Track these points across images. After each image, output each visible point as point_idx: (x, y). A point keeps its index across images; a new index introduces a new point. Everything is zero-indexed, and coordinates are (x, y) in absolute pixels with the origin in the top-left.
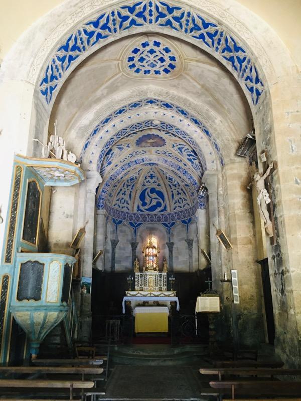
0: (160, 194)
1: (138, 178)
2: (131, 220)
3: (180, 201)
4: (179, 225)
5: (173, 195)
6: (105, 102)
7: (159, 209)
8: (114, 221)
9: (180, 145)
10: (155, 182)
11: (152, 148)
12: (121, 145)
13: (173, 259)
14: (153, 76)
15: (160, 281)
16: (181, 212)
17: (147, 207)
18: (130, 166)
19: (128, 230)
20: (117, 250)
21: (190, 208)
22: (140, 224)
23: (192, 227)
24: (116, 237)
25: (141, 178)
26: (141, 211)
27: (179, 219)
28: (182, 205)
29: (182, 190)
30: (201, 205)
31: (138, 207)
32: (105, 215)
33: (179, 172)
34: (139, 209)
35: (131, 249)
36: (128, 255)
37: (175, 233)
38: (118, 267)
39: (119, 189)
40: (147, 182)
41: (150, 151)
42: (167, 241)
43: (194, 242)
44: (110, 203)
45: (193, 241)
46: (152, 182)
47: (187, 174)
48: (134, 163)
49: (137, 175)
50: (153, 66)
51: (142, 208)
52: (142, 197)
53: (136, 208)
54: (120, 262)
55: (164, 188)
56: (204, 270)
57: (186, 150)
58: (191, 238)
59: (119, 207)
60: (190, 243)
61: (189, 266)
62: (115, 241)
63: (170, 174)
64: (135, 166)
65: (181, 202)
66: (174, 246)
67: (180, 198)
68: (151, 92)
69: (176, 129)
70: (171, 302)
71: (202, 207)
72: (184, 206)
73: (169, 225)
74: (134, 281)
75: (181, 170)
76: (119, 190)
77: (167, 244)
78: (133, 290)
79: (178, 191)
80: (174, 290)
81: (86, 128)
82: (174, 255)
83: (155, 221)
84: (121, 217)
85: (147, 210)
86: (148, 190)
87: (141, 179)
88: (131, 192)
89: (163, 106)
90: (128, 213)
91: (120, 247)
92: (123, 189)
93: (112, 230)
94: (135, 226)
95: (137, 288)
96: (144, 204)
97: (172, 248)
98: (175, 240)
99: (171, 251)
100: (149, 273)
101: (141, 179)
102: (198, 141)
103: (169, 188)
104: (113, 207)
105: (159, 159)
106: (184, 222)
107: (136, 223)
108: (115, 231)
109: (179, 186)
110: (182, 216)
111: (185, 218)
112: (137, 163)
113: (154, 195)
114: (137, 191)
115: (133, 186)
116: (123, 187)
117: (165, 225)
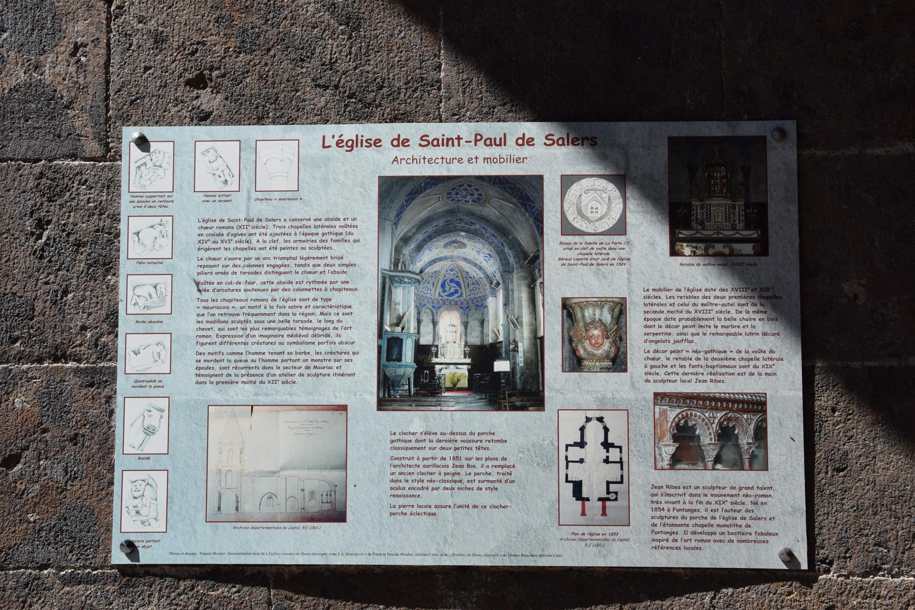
0: (458, 284)
7: (457, 295)
34: (440, 295)
50: (465, 197)
51: (442, 294)
52: (443, 286)
53: (437, 295)
98: (470, 320)
101: (443, 272)
106: (477, 306)
113: (453, 284)
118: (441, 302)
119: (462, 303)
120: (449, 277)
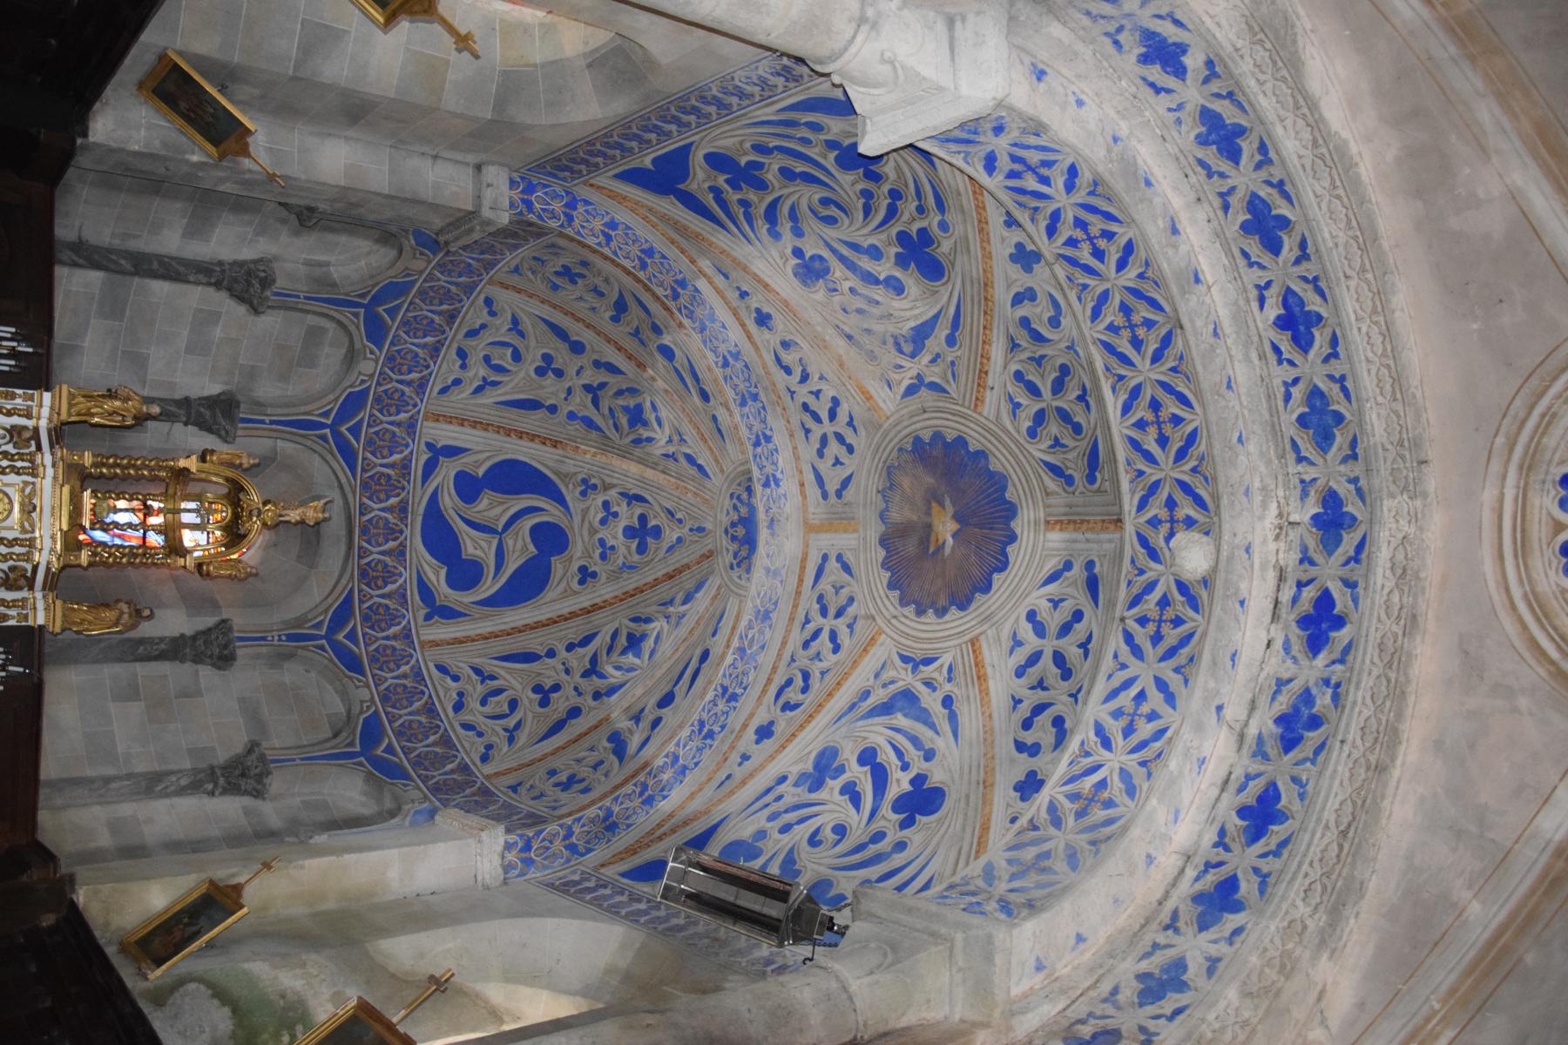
0: (527, 584)
1: (637, 452)
2: (377, 400)
3: (499, 704)
4: (344, 694)
5: (529, 657)
6: (1392, 217)
7: (437, 576)
8: (395, 290)
9: (947, 702)
10: (606, 552)
11: (874, 530)
12: (951, 341)
13: (118, 669)
14: (1539, 531)
16: (430, 710)
17: (450, 502)
18: (743, 403)
19: (319, 382)
20: (195, 296)
21: (464, 768)
22: (348, 455)
23: (348, 790)
24: (288, 303)
25: (634, 468)
26: (430, 469)
27: (385, 699)
28: (475, 712)
29: (575, 712)
30: (527, 847)
31: (453, 451)
32: (472, 215)
33: (710, 696)
36: (157, 365)
37: (291, 674)
38: (74, 287)
39: (586, 336)
40: (606, 505)
41: (840, 521)
42: (241, 621)
43: (247, 801)
44: (517, 270)
45: (258, 794)
46: (603, 533)
47: (697, 743)
48: (757, 427)
49: (658, 449)
51: (447, 472)
52: (512, 477)
53: (447, 434)
54: (113, 308)
57: (915, 741)
58: (275, 783)
59: (472, 333)
60: (242, 774)
61: (76, 782)
62: (267, 282)
63: (668, 641)
64: (744, 432)
65: (487, 709)
66: (206, 673)
67: (513, 704)
68: (1414, 518)
69: (1161, 685)
71: (511, 857)
72: (467, 727)
73: (340, 637)
75: (722, 705)
76: (578, 332)
79: (556, 688)
81: (1287, 63)
82: (142, 670)
83: (363, 553)
84: (411, 343)
85: (434, 495)
86: (551, 513)
87: (628, 472)
88: (553, 409)
89: (1309, 593)
90: (421, 386)
91: (214, 317)
92: (585, 360)
93: (336, 273)
96: (468, 487)
97: (197, 660)
99: (175, 650)
100: (49, 488)
101: (628, 472)
102: (1136, 841)
103: (573, 631)
104: (485, 289)
105: (776, 573)
106: (372, 731)
107: (356, 431)
108: (326, 295)
109: (597, 696)
110: (404, 715)
111: (399, 734)
112: (757, 444)
113: (520, 549)
114: (555, 444)
115: (589, 423)
116: (597, 364)
117: (343, 614)
118: (380, 464)
120: (581, 519)
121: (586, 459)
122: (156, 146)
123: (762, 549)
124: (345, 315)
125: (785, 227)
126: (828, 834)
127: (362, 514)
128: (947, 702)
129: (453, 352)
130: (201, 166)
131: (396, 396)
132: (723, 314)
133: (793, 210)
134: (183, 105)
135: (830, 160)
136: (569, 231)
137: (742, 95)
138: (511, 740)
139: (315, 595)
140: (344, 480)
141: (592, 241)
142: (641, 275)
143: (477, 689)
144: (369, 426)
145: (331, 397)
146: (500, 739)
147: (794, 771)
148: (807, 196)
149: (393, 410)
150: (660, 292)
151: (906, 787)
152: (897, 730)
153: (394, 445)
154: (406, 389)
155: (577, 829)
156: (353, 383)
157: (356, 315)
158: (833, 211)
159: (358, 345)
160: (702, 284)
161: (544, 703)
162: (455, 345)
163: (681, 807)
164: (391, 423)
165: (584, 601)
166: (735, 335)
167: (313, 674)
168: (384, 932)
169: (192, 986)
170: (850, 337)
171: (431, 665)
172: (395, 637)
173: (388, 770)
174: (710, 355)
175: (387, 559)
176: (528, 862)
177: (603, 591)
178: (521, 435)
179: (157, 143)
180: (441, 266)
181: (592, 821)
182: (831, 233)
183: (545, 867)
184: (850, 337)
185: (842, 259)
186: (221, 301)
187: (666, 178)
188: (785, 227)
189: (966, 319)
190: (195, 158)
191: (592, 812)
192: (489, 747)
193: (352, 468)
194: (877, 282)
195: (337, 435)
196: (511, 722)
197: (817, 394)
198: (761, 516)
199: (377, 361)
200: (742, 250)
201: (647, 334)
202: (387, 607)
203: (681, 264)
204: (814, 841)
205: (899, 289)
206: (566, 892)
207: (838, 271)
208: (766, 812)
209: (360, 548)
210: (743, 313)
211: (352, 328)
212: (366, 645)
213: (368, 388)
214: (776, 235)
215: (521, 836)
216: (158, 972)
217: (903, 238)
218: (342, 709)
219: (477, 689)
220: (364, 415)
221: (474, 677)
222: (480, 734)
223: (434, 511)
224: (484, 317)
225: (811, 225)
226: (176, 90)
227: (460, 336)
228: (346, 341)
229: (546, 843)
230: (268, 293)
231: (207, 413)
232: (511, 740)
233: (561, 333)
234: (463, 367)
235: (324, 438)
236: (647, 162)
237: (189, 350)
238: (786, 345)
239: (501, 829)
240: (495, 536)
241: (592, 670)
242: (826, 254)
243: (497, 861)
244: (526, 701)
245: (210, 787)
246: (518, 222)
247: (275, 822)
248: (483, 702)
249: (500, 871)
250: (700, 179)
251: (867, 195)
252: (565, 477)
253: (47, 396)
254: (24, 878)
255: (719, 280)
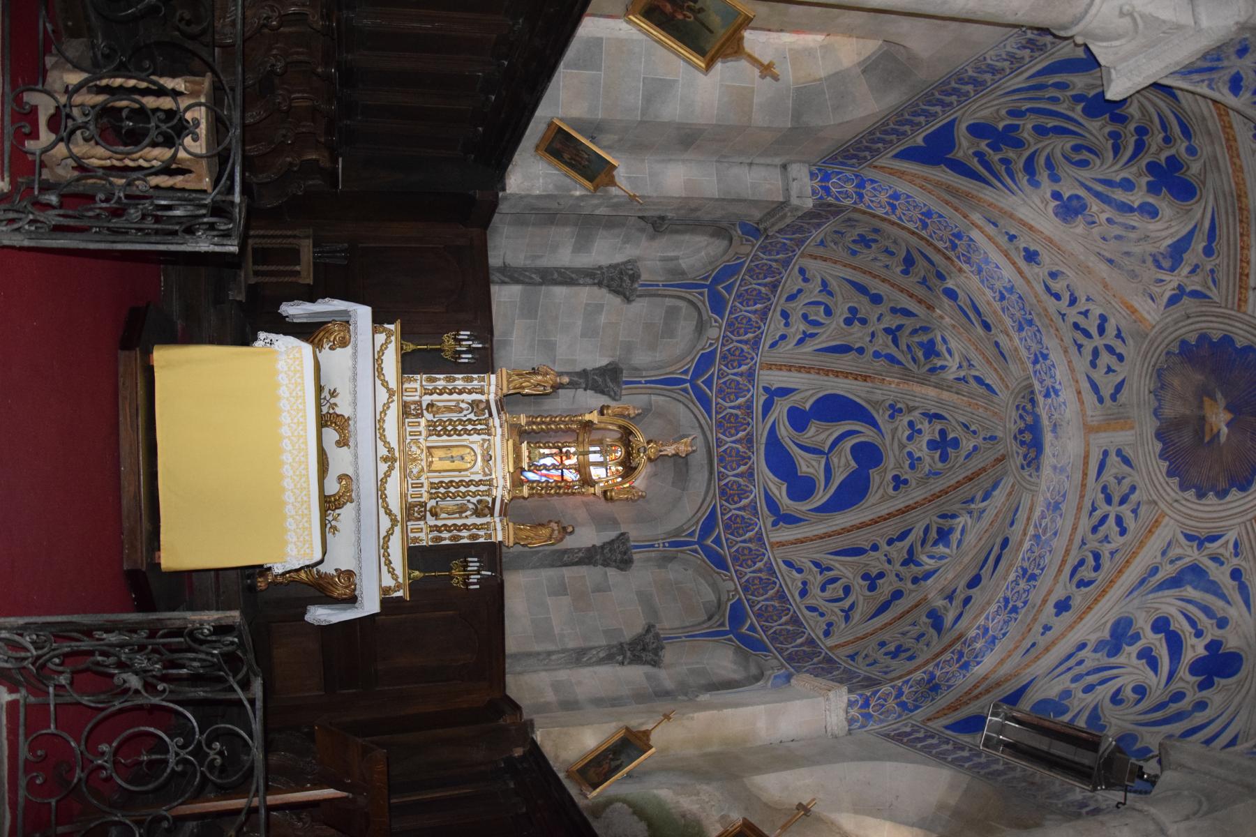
0: (852, 492)
1: (933, 378)
2: (724, 357)
3: (836, 590)
4: (714, 586)
5: (857, 552)
7: (780, 491)
8: (729, 271)
10: (914, 462)
11: (1150, 426)
12: (1208, 251)
15: (461, 510)
16: (781, 596)
17: (785, 432)
18: (1021, 329)
19: (677, 350)
20: (585, 294)
21: (811, 642)
22: (705, 401)
23: (722, 660)
24: (651, 292)
25: (932, 392)
27: (746, 589)
28: (816, 597)
29: (897, 595)
30: (866, 704)
31: (785, 392)
32: (783, 205)
33: (1012, 577)
34: (775, 394)
35: (589, 367)
36: (562, 351)
37: (673, 573)
38: (504, 297)
40: (911, 424)
43: (648, 669)
44: (822, 243)
45: (655, 663)
48: (1035, 347)
49: (951, 374)
51: (781, 409)
52: (833, 408)
53: (779, 379)
54: (529, 309)
55: (884, 509)
56: (535, 751)
57: (1207, 610)
58: (668, 655)
59: (791, 298)
60: (643, 649)
61: (529, 655)
62: (634, 277)
63: (972, 533)
64: (1024, 353)
65: (827, 594)
66: (612, 573)
67: (847, 590)
70: (350, 574)
72: (812, 609)
73: (709, 542)
74: (452, 366)
75: (1023, 584)
76: (876, 287)
77: (623, 537)
78: (409, 364)
79: (881, 575)
80: (414, 586)
82: (567, 572)
83: (722, 476)
84: (745, 311)
85: (773, 430)
86: (867, 434)
87: (926, 395)
88: (861, 351)
90: (756, 344)
91: (599, 308)
92: (882, 308)
93: (684, 264)
94: (697, 381)
95: (418, 382)
97: (606, 564)
98: (642, 575)
99: (589, 557)
100: (500, 443)
103: (892, 528)
104: (798, 262)
105: (1062, 470)
106: (737, 615)
107: (709, 383)
108: (679, 282)
109: (915, 580)
112: (1035, 362)
113: (844, 464)
114: (865, 378)
115: (891, 359)
116: (894, 310)
117: (709, 524)
119: (737, 526)
121: (891, 388)
122: (551, 189)
123: (1048, 450)
124: (693, 295)
125: (1043, 176)
126: (1128, 693)
127: (718, 446)
128: (1236, 574)
129: (778, 313)
130: (581, 198)
131: (737, 353)
132: (996, 256)
133: (1048, 159)
134: (566, 156)
135: (1077, 112)
136: (861, 206)
137: (993, 70)
138: (847, 618)
139: (687, 511)
140: (703, 422)
141: (880, 212)
142: (923, 233)
143: (817, 579)
144: (719, 378)
145: (689, 359)
146: (838, 618)
147: (1093, 639)
148: (1060, 146)
149: (735, 364)
150: (940, 245)
151: (1201, 651)
152: (1189, 601)
153: (739, 391)
154: (745, 347)
155: (906, 690)
156: (703, 347)
157: (701, 294)
158: (1085, 155)
159: (705, 317)
160: (975, 234)
161: (872, 588)
162: (779, 309)
163: (994, 671)
164: (735, 374)
165: (900, 503)
166: (1008, 272)
167: (690, 572)
168: (758, 769)
169: (619, 805)
170: (1110, 261)
171: (780, 561)
172: (750, 540)
173: (751, 644)
174: (988, 292)
175: (740, 480)
176: (867, 717)
177: (915, 494)
178: (837, 374)
179: (551, 186)
180: (763, 249)
181: (918, 683)
182: (1084, 174)
183: (881, 721)
184: (1110, 261)
185: (1098, 195)
186: (603, 296)
187: (937, 150)
188: (1043, 176)
189: (1222, 231)
190: (578, 193)
191: (918, 675)
192: (830, 625)
193: (709, 412)
194: (1131, 209)
195: (695, 387)
196: (846, 604)
197: (1085, 314)
198: (1045, 422)
199: (720, 328)
200: (1008, 201)
201: (934, 281)
202: (743, 517)
203: (955, 220)
204: (1116, 699)
205: (1152, 212)
206: (901, 742)
207: (1095, 206)
208: (1070, 675)
209: (719, 473)
210: (1013, 254)
211: (700, 304)
212: (729, 548)
213: (716, 349)
214: (1035, 184)
215: (861, 695)
216: (595, 793)
217: (1152, 167)
218: (712, 597)
219: (817, 579)
220: (714, 370)
221: (815, 569)
222: (822, 615)
223: (773, 441)
224: (800, 284)
225: (1066, 170)
226: (561, 146)
227: (783, 300)
228: (696, 314)
229: (881, 701)
230: (636, 285)
231: (600, 380)
232: (847, 618)
233: (862, 289)
234: (787, 324)
235: (685, 390)
236: (919, 140)
237: (583, 335)
238: (1053, 275)
239: (845, 689)
240: (824, 455)
241: (910, 559)
242: (1082, 192)
243: (842, 715)
244: (857, 587)
245: (620, 658)
246: (820, 205)
247: (669, 684)
248: (823, 589)
249: (845, 724)
250: (965, 147)
251: (1115, 136)
252: (876, 404)
253: (493, 377)
254: (501, 722)
255: (990, 229)
